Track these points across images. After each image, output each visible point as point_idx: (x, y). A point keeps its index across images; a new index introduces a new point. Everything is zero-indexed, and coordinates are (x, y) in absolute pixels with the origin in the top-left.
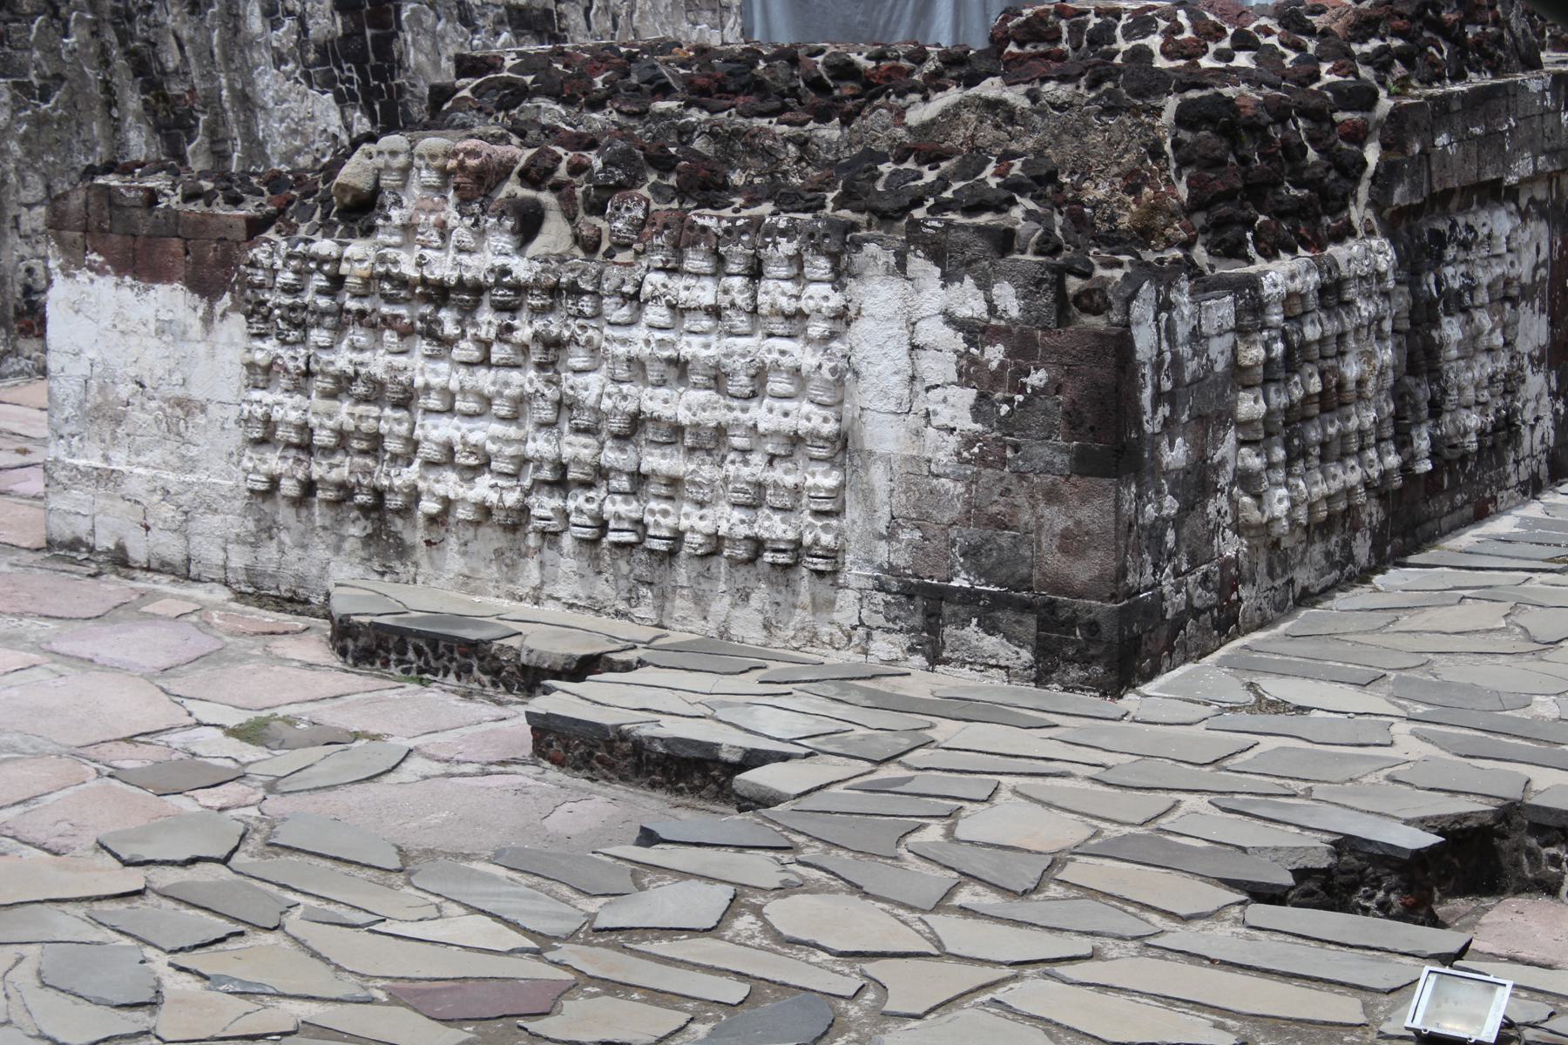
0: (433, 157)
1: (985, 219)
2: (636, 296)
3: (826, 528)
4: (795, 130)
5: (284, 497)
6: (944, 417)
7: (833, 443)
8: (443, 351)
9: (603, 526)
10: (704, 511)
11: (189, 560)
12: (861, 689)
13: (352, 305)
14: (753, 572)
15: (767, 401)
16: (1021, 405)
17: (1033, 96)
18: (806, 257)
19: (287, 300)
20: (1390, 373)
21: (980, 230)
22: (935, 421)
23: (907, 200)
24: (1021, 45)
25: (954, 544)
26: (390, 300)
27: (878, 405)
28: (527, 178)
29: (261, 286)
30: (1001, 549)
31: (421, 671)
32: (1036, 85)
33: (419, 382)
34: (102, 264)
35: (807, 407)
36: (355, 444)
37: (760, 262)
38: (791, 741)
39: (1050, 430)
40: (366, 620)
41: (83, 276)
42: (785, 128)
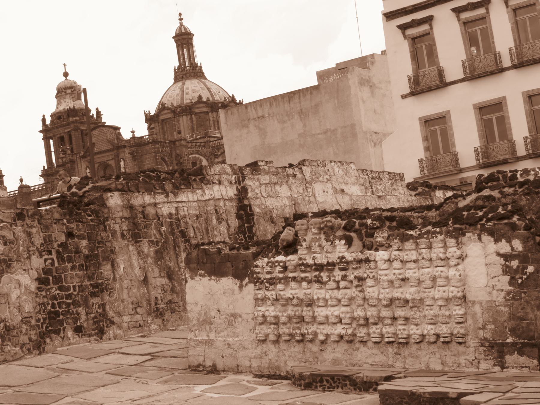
0: (316, 224)
1: (505, 221)
2: (389, 260)
3: (461, 327)
5: (270, 341)
6: (499, 287)
7: (461, 299)
8: (323, 286)
9: (382, 336)
10: (418, 327)
11: (238, 366)
12: (484, 377)
13: (291, 275)
14: (436, 346)
15: (437, 288)
16: (525, 279)
17: (501, 193)
18: (447, 240)
19: (268, 276)
21: (506, 224)
22: (496, 288)
25: (506, 328)
28: (345, 228)
29: (259, 273)
30: (523, 327)
31: (329, 388)
32: (502, 189)
33: (315, 297)
34: (204, 274)
35: (452, 289)
36: (294, 320)
37: (431, 243)
40: (309, 373)
41: (198, 278)
42: (417, 214)
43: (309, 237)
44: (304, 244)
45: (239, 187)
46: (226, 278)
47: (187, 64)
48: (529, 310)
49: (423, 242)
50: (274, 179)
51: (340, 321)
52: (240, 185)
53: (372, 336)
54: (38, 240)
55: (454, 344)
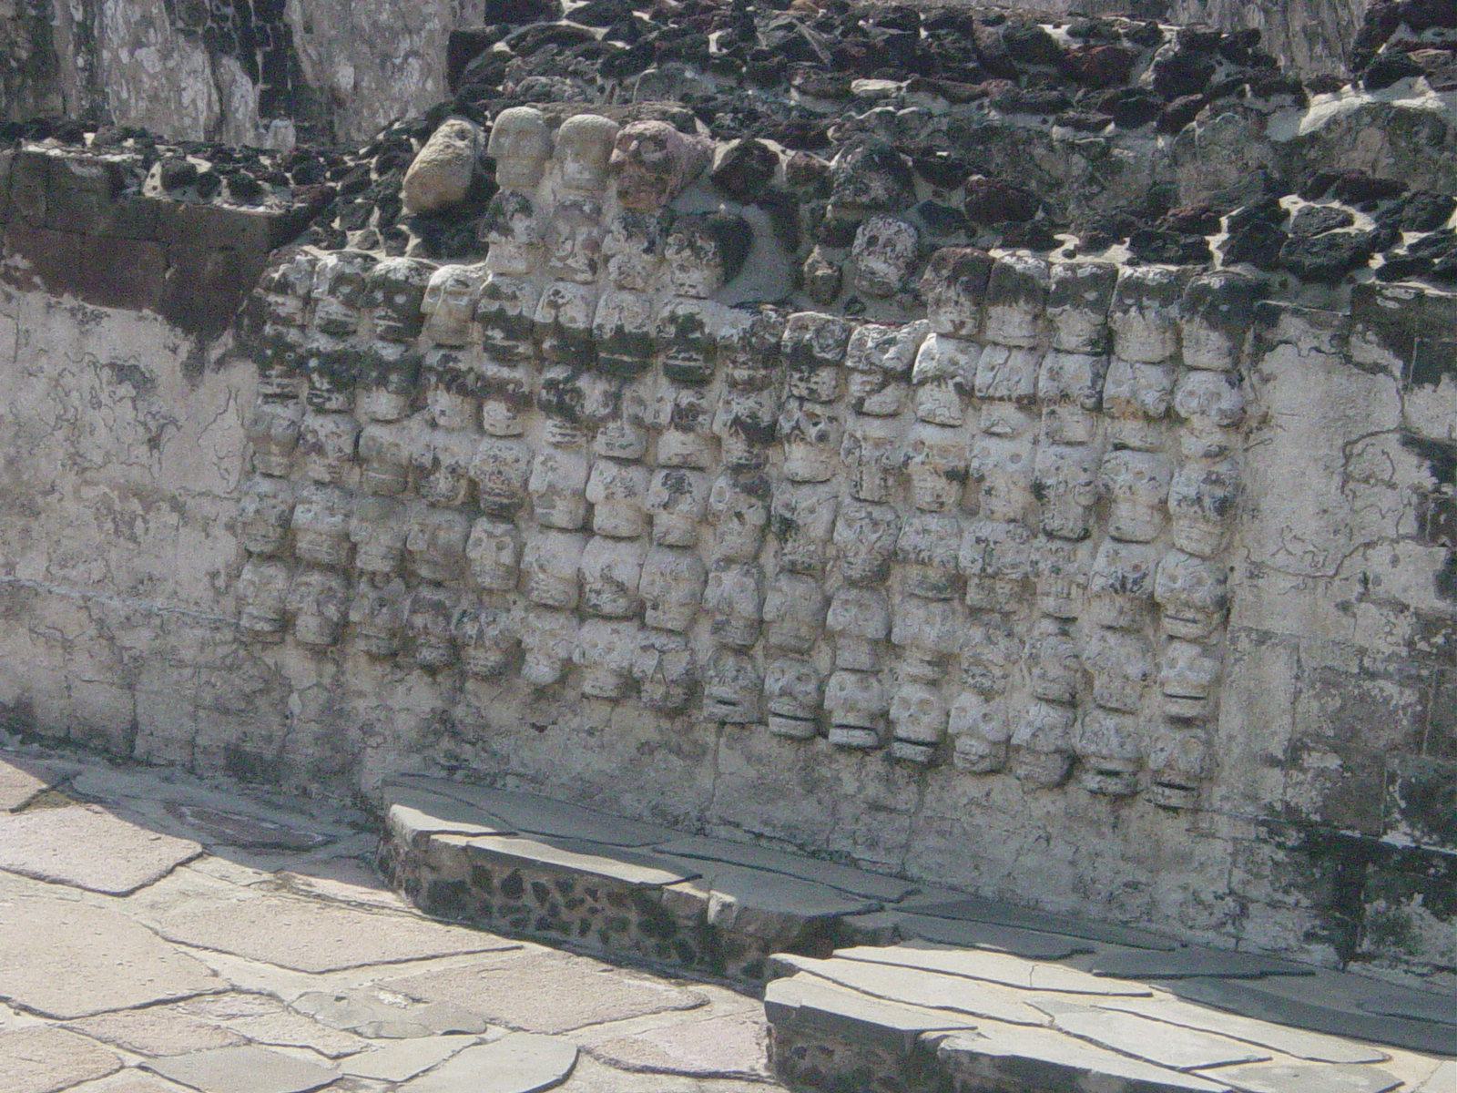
4: (1084, 138)
7: (1209, 616)
9: (819, 722)
14: (1061, 804)
23: (1346, 255)
24: (1417, 28)
25: (1392, 779)
26: (503, 356)
27: (1281, 558)
29: (287, 321)
34: (28, 274)
38: (1186, 1071)
44: (520, 225)
46: (133, 314)
49: (1075, 326)
51: (637, 614)
53: (773, 706)
55: (1141, 805)
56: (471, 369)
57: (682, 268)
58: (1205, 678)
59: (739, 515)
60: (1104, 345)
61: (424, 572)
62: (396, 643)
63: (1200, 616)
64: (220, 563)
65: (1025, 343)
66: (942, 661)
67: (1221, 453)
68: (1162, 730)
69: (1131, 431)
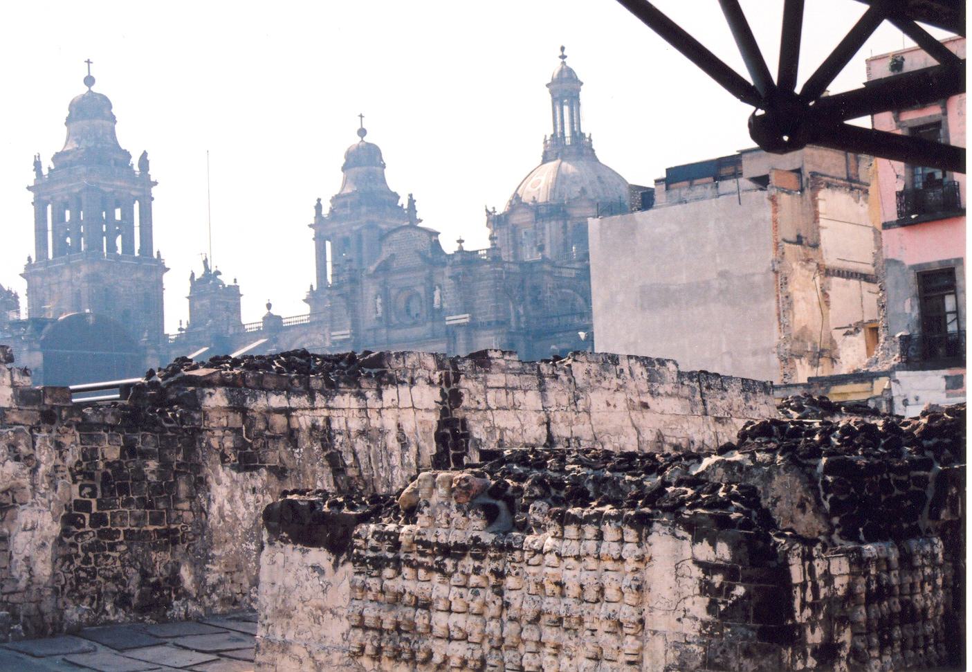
5: (368, 655)
7: (637, 626)
8: (446, 580)
17: (753, 458)
19: (371, 554)
20: (942, 607)
22: (689, 614)
24: (753, 439)
26: (423, 554)
27: (658, 605)
29: (360, 548)
34: (287, 538)
39: (747, 618)
43: (434, 500)
44: (426, 510)
45: (446, 391)
47: (567, 133)
48: (731, 655)
49: (590, 531)
50: (513, 380)
51: (465, 638)
52: (448, 385)
54: (72, 457)
56: (414, 559)
57: (474, 521)
58: (637, 647)
59: (494, 602)
60: (600, 537)
61: (402, 628)
62: (396, 653)
63: (634, 626)
64: (344, 631)
65: (575, 537)
66: (557, 647)
67: (637, 570)
68: (625, 666)
69: (609, 565)
